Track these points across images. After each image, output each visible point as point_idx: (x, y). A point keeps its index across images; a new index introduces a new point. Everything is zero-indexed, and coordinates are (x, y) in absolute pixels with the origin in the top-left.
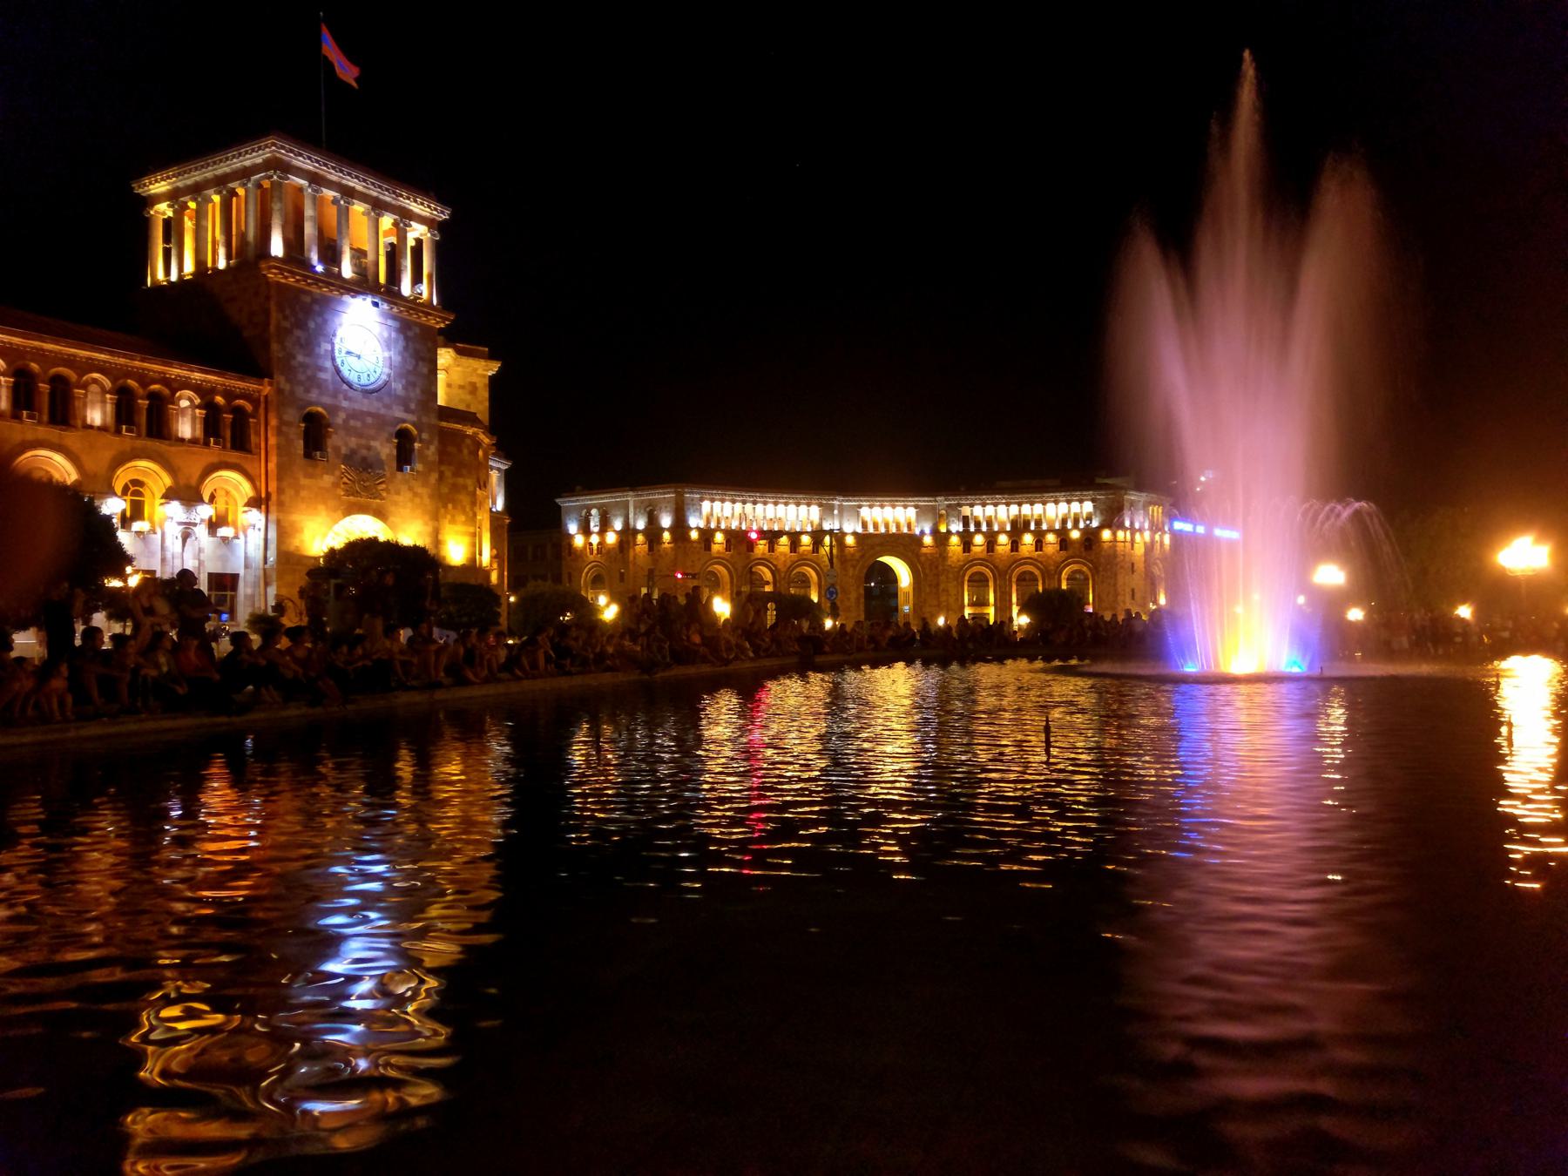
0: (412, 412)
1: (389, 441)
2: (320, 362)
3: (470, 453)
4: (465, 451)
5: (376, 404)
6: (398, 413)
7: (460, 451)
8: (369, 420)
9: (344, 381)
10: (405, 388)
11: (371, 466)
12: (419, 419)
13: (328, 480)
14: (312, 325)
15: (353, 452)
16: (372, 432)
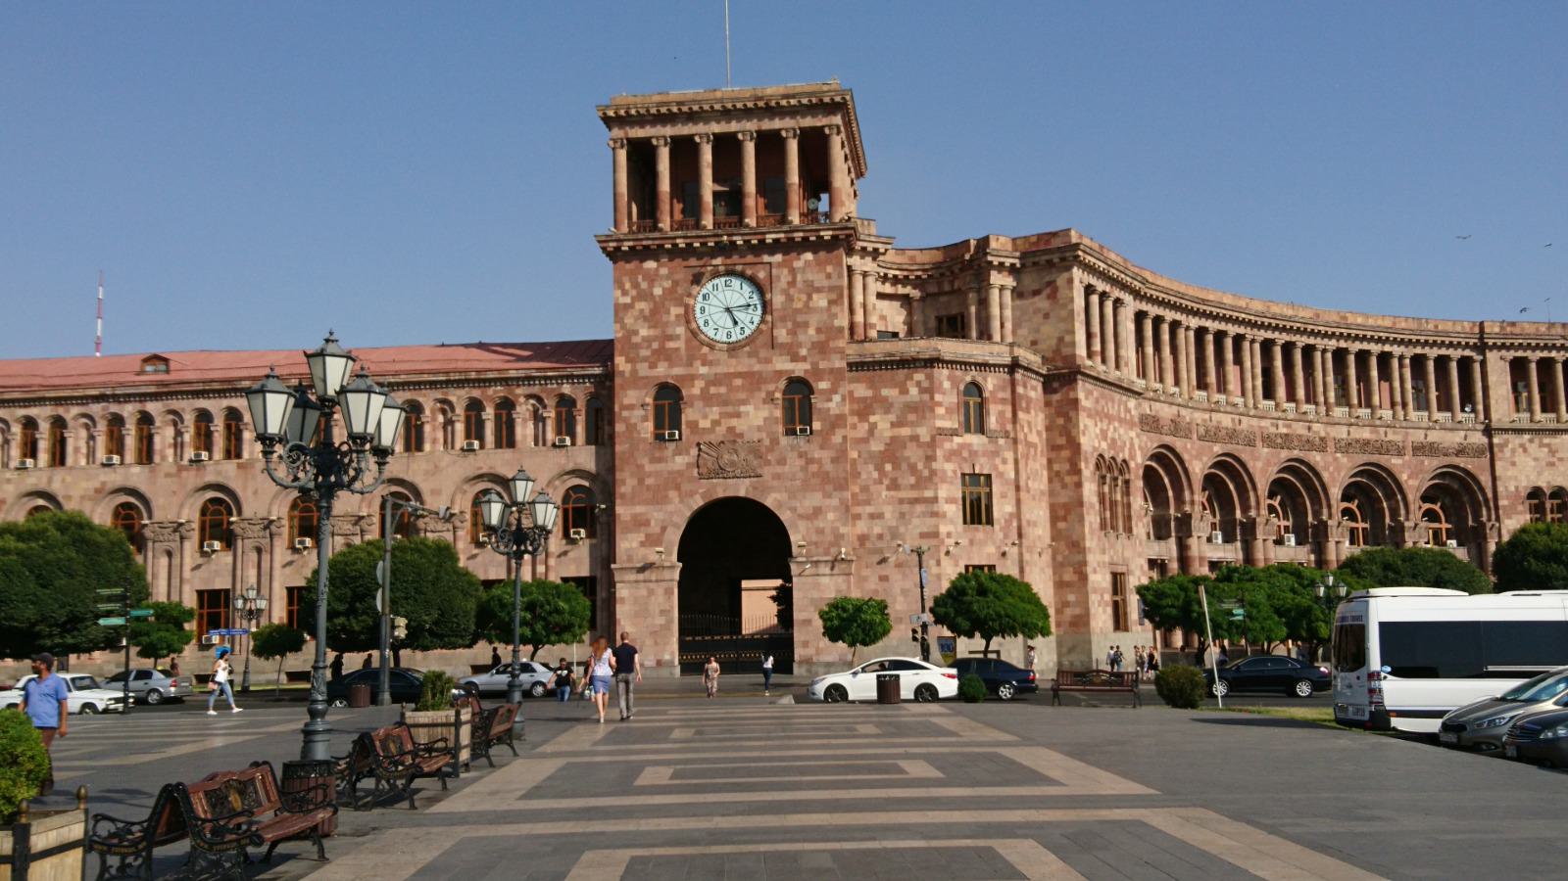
0: (804, 359)
1: (765, 402)
2: (669, 331)
3: (922, 390)
4: (914, 391)
5: (746, 361)
6: (783, 364)
7: (904, 391)
8: (738, 382)
9: (702, 343)
10: (793, 333)
11: (741, 435)
12: (815, 365)
13: (681, 461)
14: (658, 291)
15: (716, 423)
16: (742, 396)
